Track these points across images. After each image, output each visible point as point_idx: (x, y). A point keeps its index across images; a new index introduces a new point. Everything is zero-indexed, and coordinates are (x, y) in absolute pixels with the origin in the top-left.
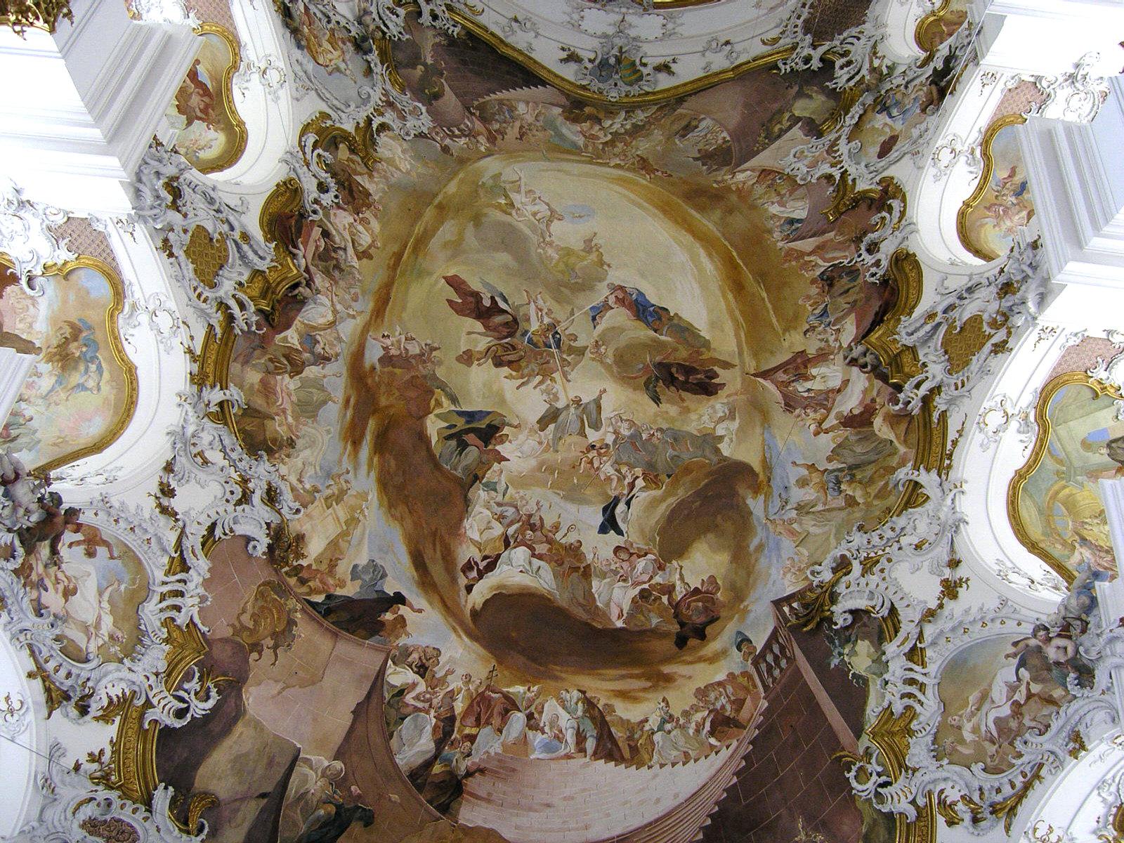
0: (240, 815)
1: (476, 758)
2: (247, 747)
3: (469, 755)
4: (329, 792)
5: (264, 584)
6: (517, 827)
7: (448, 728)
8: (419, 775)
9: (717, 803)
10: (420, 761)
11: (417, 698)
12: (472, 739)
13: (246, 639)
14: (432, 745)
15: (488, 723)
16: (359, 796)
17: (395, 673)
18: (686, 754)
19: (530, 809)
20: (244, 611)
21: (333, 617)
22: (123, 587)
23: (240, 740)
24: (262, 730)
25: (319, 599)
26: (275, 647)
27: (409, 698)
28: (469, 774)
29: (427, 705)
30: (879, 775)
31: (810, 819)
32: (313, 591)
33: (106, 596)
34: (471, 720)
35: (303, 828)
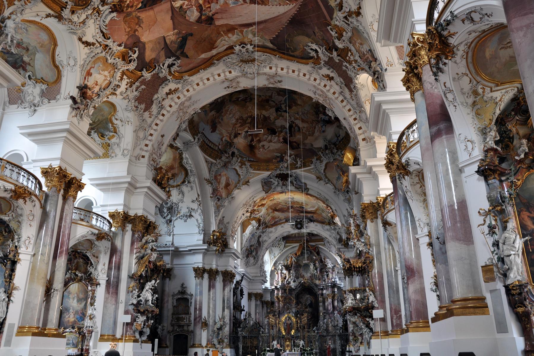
0: (161, 56)
1: (213, 11)
2: (151, 46)
3: (211, 11)
4: (178, 36)
5: (124, 19)
6: (233, 22)
7: (201, 8)
8: (199, 20)
9: (292, 16)
10: (197, 18)
11: (187, 5)
12: (210, 7)
13: (131, 33)
14: (199, 13)
15: (212, 2)
16: (186, 33)
17: (176, 4)
18: (280, 4)
19: (236, 17)
20: (125, 29)
21: (148, 5)
22: (101, 66)
23: (148, 47)
24: (152, 41)
25: (140, 5)
26: (140, 26)
27: (184, 7)
28: (213, 15)
29: (191, 6)
30: (336, 33)
31: (318, 28)
32: (136, 6)
33: (101, 72)
34: (207, 3)
35: (177, 46)
